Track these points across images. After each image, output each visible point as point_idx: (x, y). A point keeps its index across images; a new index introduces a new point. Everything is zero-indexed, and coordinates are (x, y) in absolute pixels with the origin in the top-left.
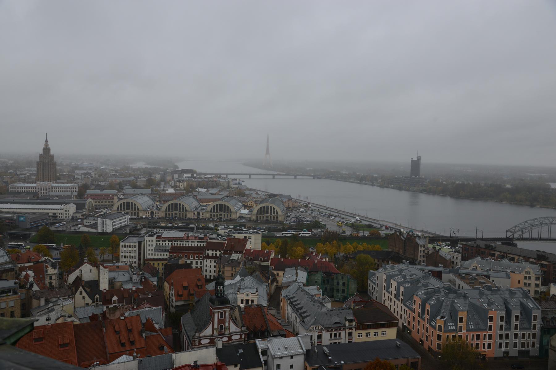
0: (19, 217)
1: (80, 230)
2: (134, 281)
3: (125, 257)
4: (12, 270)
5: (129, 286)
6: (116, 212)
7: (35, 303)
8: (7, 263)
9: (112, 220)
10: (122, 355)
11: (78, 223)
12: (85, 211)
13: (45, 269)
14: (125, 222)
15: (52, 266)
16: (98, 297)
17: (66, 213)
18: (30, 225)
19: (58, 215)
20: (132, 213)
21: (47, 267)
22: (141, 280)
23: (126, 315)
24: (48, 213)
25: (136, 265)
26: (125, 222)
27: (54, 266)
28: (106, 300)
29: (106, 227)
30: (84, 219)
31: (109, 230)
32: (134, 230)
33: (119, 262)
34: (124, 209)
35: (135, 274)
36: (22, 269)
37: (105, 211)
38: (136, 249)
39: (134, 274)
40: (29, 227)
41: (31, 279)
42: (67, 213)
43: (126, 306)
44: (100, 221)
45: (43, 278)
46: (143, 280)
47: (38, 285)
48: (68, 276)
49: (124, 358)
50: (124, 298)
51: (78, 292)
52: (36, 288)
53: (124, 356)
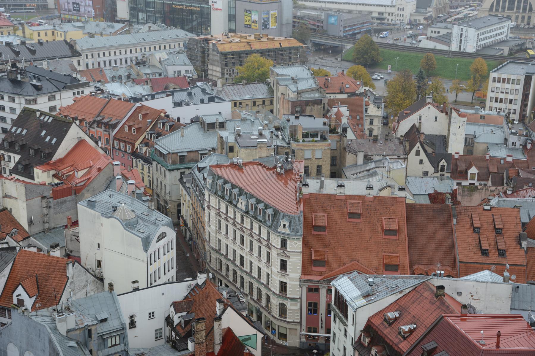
0: (328, 16)
1: (421, 45)
2: (510, 146)
3: (496, 100)
4: (319, 102)
5: (500, 153)
6: (487, 14)
7: (349, 158)
8: (312, 90)
9: (478, 29)
10: (482, 269)
11: (418, 32)
12: (431, 12)
13: (364, 107)
14: (502, 33)
15: (375, 103)
16: (445, 164)
17: (400, 12)
18: (344, 32)
19: (385, 15)
20: (517, 17)
21: (367, 104)
22: (525, 146)
23: (493, 202)
24: (371, 13)
25: (516, 117)
26: (502, 33)
27: (377, 101)
28: (459, 174)
29: (466, 41)
30: (429, 25)
31: (471, 48)
32: (518, 51)
33: (484, 108)
34: (503, 8)
35: (515, 134)
36: (332, 103)
37: (466, 11)
38: (520, 87)
39: (512, 133)
40: (341, 34)
41: (344, 120)
42: (402, 13)
43: (493, 188)
44: (456, 30)
45: (360, 122)
46: (529, 146)
47: (354, 131)
48: (398, 122)
49: (485, 275)
50: (489, 173)
51: (413, 151)
52: (350, 135)
53: (487, 272)
